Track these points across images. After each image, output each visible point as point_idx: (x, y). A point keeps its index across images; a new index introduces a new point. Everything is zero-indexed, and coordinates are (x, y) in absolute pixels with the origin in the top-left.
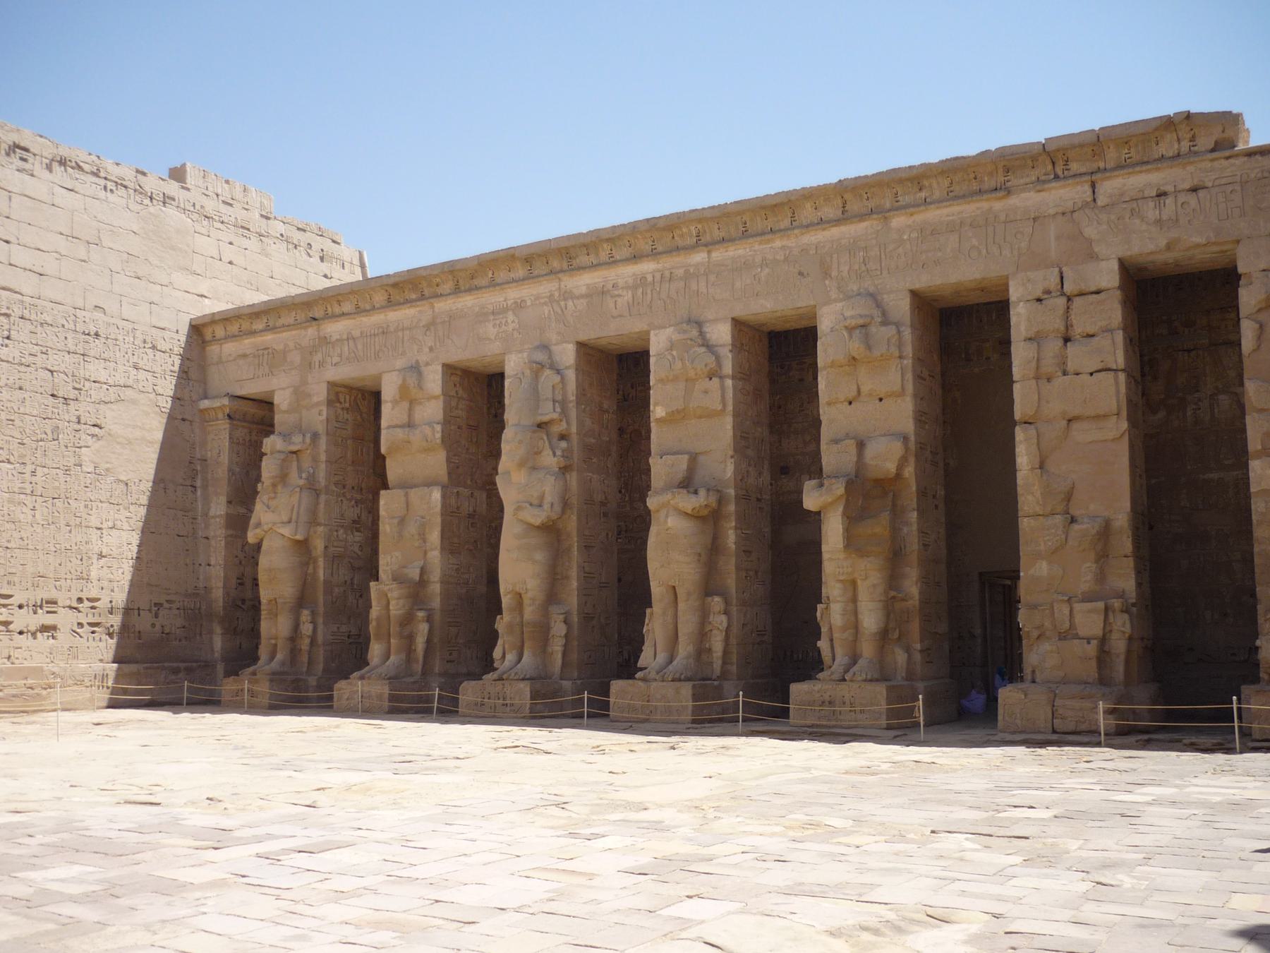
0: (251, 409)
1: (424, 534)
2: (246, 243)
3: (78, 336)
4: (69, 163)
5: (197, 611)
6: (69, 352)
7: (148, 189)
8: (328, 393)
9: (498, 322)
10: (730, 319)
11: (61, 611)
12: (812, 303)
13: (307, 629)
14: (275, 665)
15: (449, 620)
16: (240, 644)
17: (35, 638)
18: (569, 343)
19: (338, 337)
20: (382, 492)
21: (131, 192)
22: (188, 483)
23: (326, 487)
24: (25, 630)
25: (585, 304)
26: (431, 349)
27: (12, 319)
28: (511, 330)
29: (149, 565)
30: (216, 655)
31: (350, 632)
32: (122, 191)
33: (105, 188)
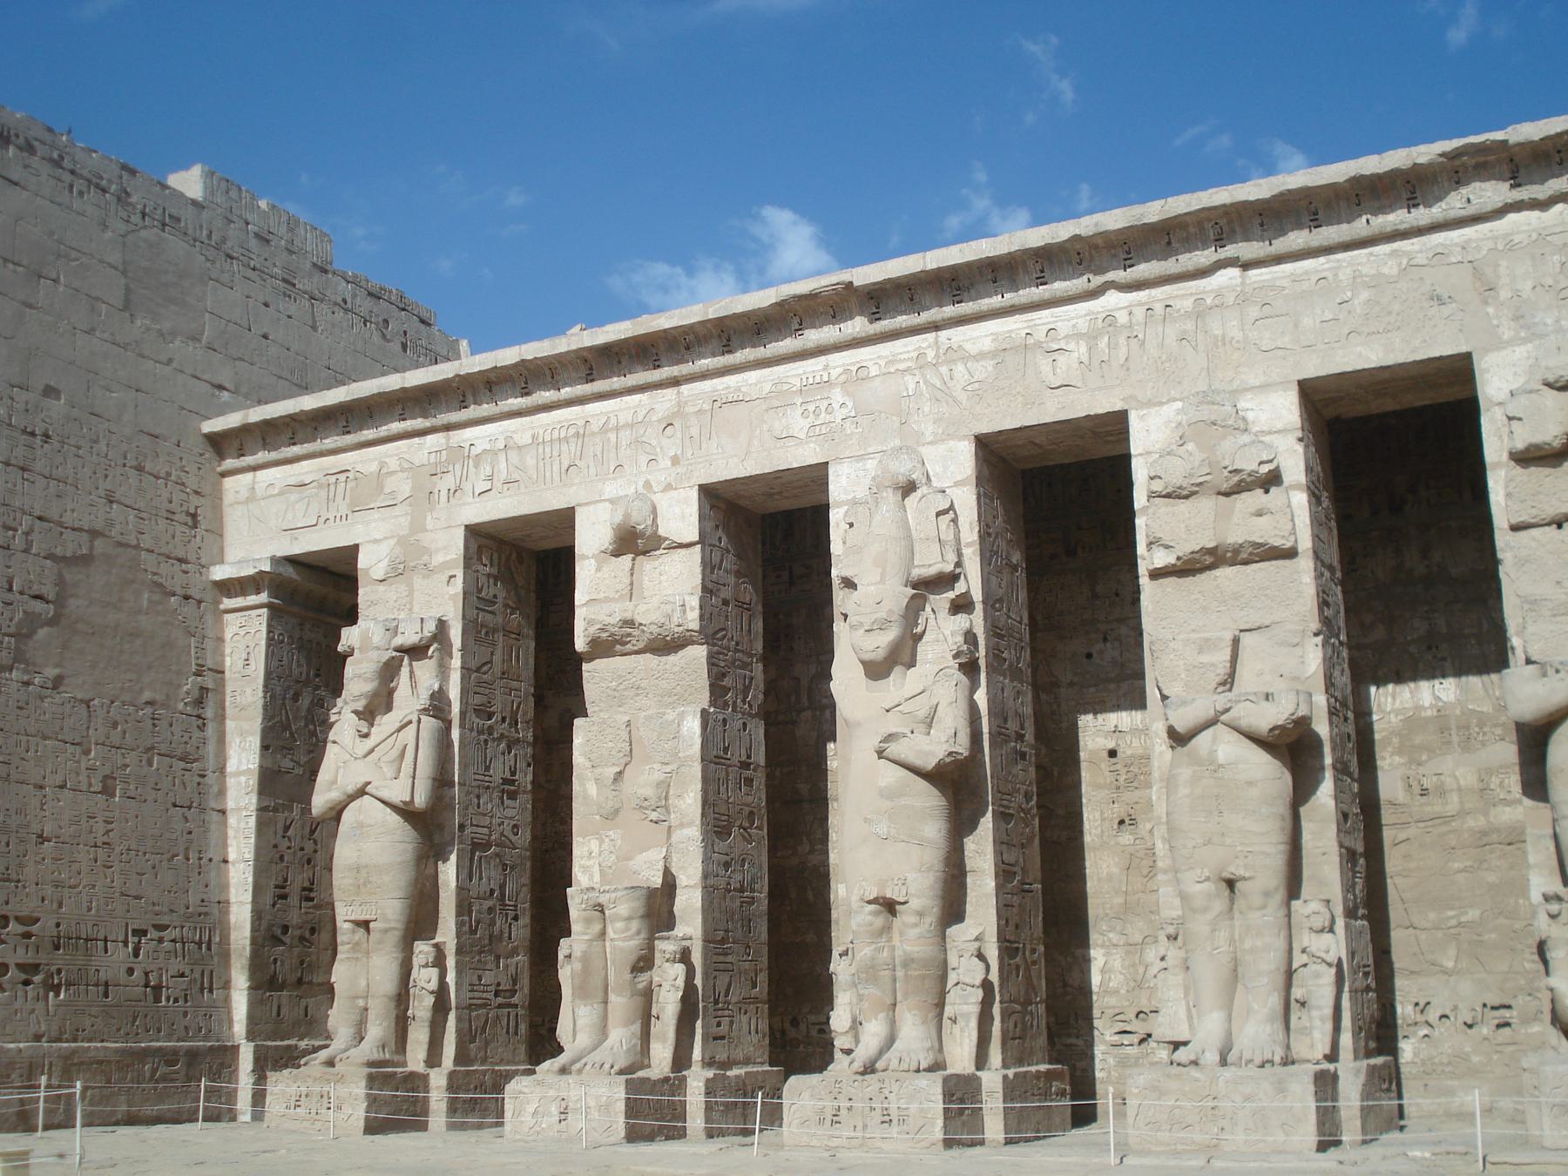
1: (666, 798)
2: (293, 309)
3: (14, 434)
4: (13, 138)
9: (811, 408)
12: (1464, 349)
13: (425, 977)
14: (369, 1048)
15: (716, 958)
18: (965, 437)
20: (578, 722)
25: (990, 369)
26: (675, 461)
28: (839, 420)
31: (499, 984)
33: (71, 187)
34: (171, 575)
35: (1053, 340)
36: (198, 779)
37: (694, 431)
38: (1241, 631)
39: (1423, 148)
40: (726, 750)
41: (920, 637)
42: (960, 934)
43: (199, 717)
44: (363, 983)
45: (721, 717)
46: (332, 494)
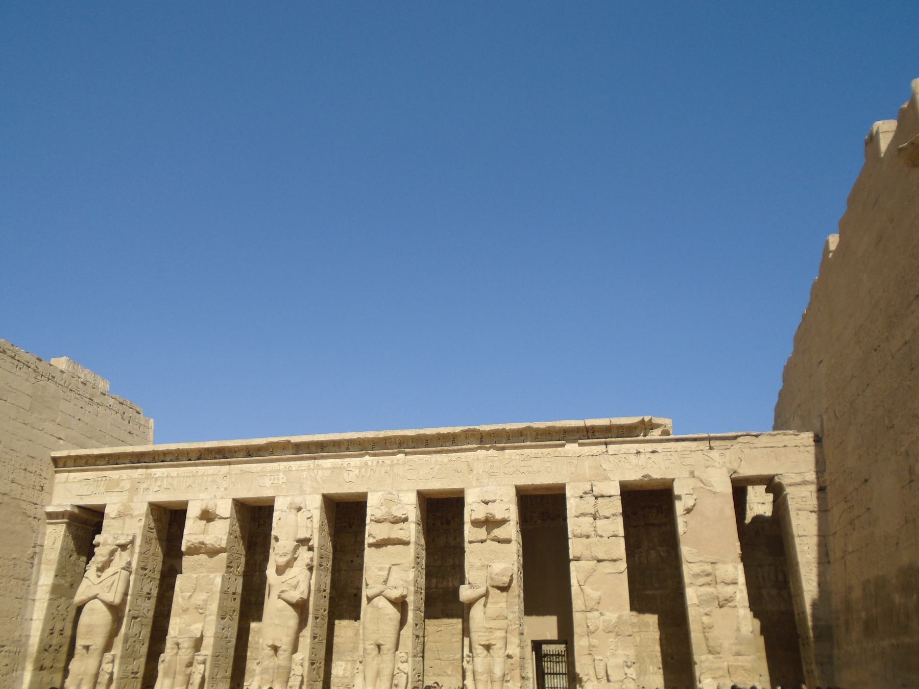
0: (85, 516)
7: (40, 369)
9: (273, 477)
10: (416, 492)
12: (463, 487)
13: (107, 667)
18: (318, 494)
19: (161, 475)
23: (137, 569)
26: (226, 489)
34: (30, 509)
35: (349, 467)
36: (27, 588)
37: (233, 480)
38: (392, 565)
39: (457, 428)
40: (228, 588)
41: (296, 559)
42: (298, 657)
43: (31, 563)
45: (228, 577)
46: (99, 484)
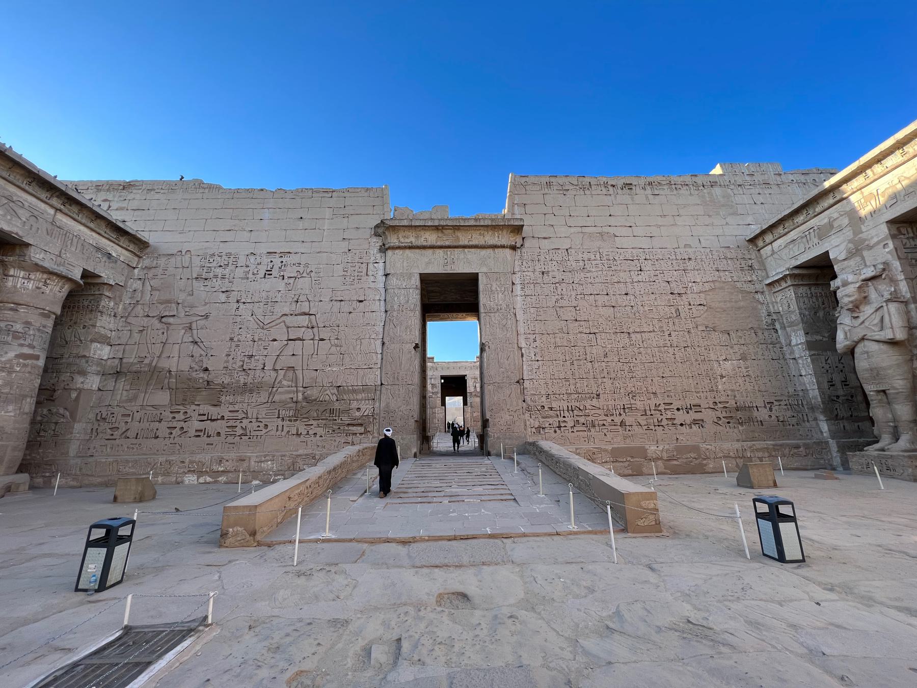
2: (769, 191)
4: (653, 184)
5: (801, 406)
6: (676, 271)
7: (700, 183)
8: (889, 230)
11: (703, 410)
16: (844, 426)
17: (691, 428)
21: (691, 186)
22: (772, 328)
24: (684, 423)
27: (640, 261)
29: (757, 379)
30: (825, 435)
32: (685, 188)
44: (890, 416)
46: (808, 238)
